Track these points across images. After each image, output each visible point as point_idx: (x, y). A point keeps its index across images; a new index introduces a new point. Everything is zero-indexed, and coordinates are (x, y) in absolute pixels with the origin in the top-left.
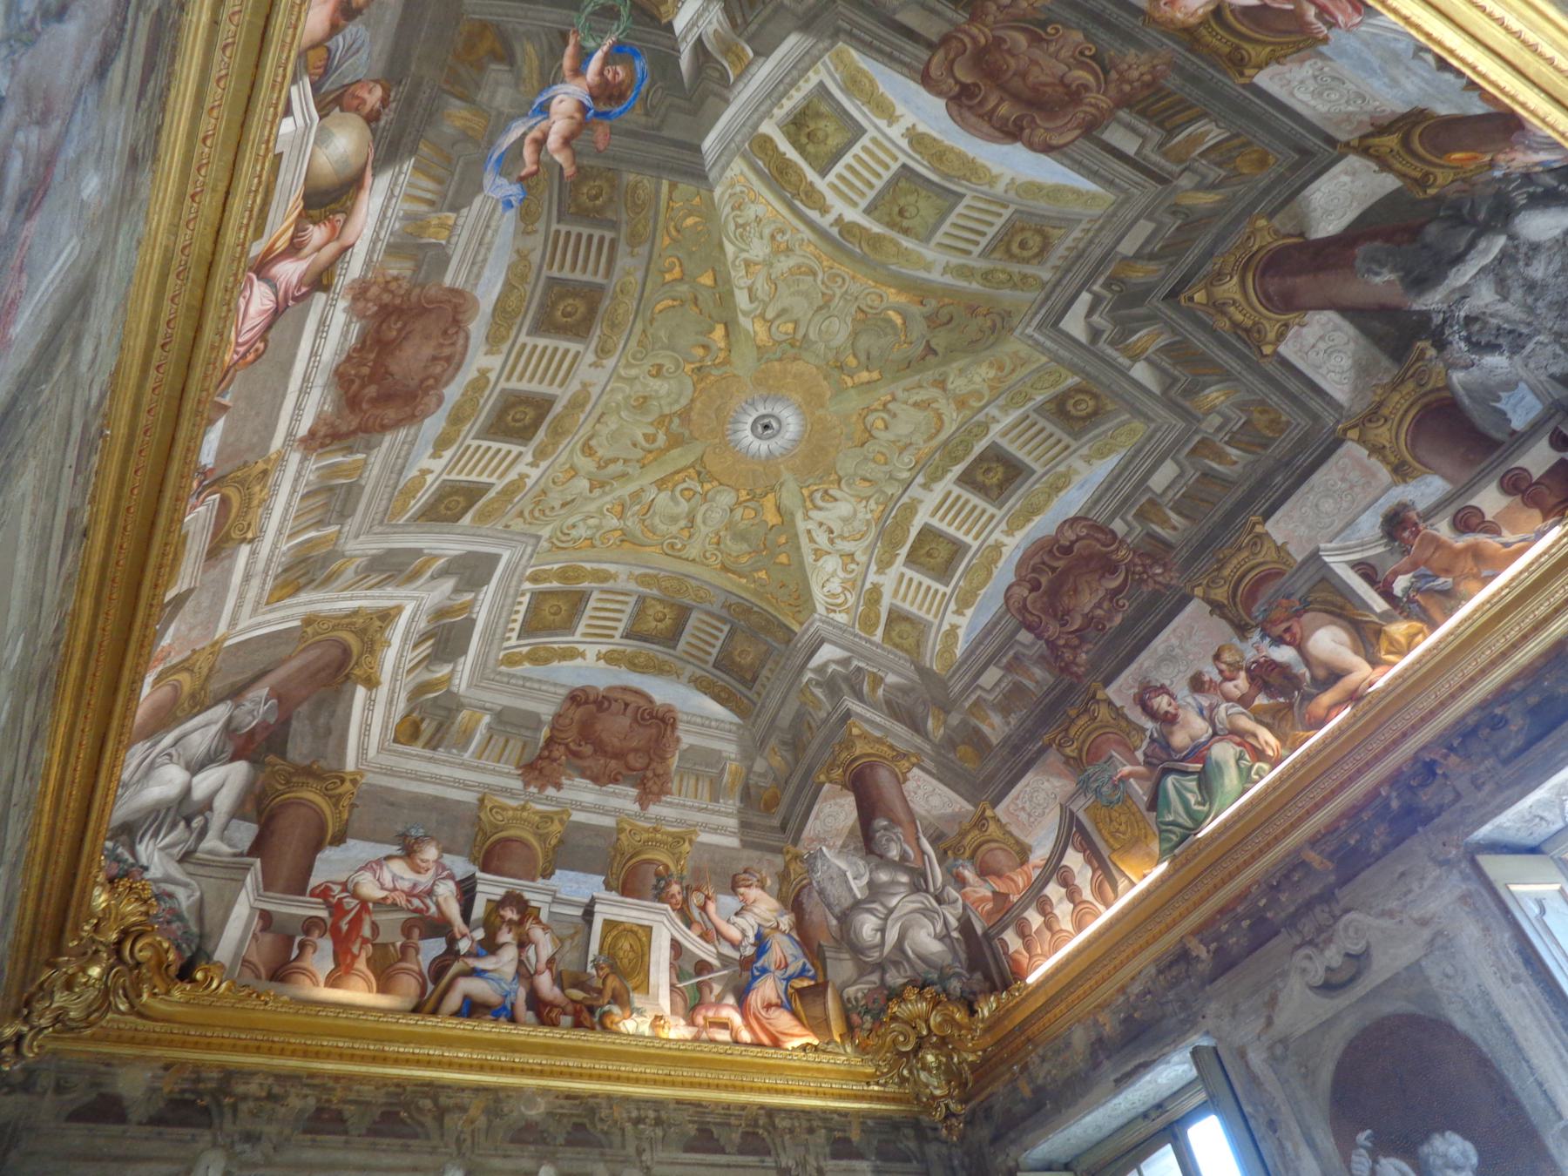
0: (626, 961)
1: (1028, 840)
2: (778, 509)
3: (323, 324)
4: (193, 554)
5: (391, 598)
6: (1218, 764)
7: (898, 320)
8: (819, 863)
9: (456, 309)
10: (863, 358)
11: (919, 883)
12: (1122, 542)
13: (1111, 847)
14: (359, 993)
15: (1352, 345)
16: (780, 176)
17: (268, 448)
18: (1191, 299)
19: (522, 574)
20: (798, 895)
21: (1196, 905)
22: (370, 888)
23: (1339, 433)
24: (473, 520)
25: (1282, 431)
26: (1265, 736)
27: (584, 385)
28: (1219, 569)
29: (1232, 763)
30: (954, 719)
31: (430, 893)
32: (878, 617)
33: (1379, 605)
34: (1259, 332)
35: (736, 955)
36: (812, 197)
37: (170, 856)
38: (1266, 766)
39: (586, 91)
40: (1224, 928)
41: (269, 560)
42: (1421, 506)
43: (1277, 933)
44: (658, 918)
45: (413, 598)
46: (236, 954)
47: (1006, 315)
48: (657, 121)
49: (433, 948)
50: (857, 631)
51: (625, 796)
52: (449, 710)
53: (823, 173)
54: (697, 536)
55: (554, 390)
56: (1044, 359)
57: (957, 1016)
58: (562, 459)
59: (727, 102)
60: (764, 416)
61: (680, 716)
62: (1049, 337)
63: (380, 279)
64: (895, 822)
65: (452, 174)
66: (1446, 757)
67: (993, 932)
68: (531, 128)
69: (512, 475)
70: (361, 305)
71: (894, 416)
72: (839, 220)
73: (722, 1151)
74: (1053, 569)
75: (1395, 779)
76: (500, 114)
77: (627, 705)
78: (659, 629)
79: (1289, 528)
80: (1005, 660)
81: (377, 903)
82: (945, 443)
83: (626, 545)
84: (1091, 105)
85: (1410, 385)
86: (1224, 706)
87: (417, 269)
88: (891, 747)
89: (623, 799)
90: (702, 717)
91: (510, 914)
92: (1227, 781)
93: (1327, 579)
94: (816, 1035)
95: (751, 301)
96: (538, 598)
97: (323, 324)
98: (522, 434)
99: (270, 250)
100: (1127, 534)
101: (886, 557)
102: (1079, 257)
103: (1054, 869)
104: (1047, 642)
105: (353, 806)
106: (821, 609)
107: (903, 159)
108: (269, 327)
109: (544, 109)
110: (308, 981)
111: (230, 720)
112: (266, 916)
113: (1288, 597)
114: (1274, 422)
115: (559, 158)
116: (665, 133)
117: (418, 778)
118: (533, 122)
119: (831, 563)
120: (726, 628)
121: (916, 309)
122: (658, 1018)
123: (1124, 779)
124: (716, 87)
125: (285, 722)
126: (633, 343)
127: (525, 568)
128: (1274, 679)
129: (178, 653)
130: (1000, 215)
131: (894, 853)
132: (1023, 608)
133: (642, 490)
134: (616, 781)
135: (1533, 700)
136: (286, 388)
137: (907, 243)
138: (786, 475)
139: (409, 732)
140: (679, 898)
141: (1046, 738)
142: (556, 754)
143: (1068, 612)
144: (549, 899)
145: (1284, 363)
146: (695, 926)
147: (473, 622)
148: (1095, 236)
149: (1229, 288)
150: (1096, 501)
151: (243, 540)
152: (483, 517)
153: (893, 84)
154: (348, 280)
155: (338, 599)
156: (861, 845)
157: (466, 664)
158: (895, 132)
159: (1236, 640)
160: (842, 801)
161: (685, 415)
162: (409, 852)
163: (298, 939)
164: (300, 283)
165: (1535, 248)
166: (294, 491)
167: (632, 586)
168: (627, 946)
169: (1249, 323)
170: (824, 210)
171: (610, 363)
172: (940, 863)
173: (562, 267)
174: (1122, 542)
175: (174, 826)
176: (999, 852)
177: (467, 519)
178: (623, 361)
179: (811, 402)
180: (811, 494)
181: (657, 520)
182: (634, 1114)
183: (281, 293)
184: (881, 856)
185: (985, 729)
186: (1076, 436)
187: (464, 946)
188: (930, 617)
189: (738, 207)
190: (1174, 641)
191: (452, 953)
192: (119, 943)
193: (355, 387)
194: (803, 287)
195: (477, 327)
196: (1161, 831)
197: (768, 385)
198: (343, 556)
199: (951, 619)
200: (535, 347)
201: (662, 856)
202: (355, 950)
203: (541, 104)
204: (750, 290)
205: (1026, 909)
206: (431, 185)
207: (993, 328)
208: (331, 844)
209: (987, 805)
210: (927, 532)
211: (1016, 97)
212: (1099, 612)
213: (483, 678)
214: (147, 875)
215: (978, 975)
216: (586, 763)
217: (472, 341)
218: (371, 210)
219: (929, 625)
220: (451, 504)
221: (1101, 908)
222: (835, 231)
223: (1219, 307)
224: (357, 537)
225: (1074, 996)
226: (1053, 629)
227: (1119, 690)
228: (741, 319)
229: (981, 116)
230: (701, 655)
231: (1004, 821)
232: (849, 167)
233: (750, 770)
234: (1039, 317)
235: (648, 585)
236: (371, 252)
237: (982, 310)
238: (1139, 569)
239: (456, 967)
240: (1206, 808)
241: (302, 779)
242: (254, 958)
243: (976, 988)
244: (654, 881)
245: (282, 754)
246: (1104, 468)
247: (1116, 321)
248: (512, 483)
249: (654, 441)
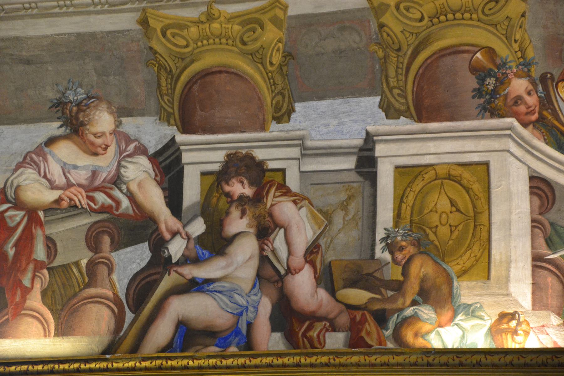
0: (444, 231)
31: (117, 180)
44: (495, 144)
49: (132, 259)
81: (49, 209)
91: (240, 188)
140: (532, 100)
144: (295, 152)
162: (75, 128)
168: (444, 204)
187: (176, 249)
191: (160, 263)
202: (26, 282)
244: (472, 83)
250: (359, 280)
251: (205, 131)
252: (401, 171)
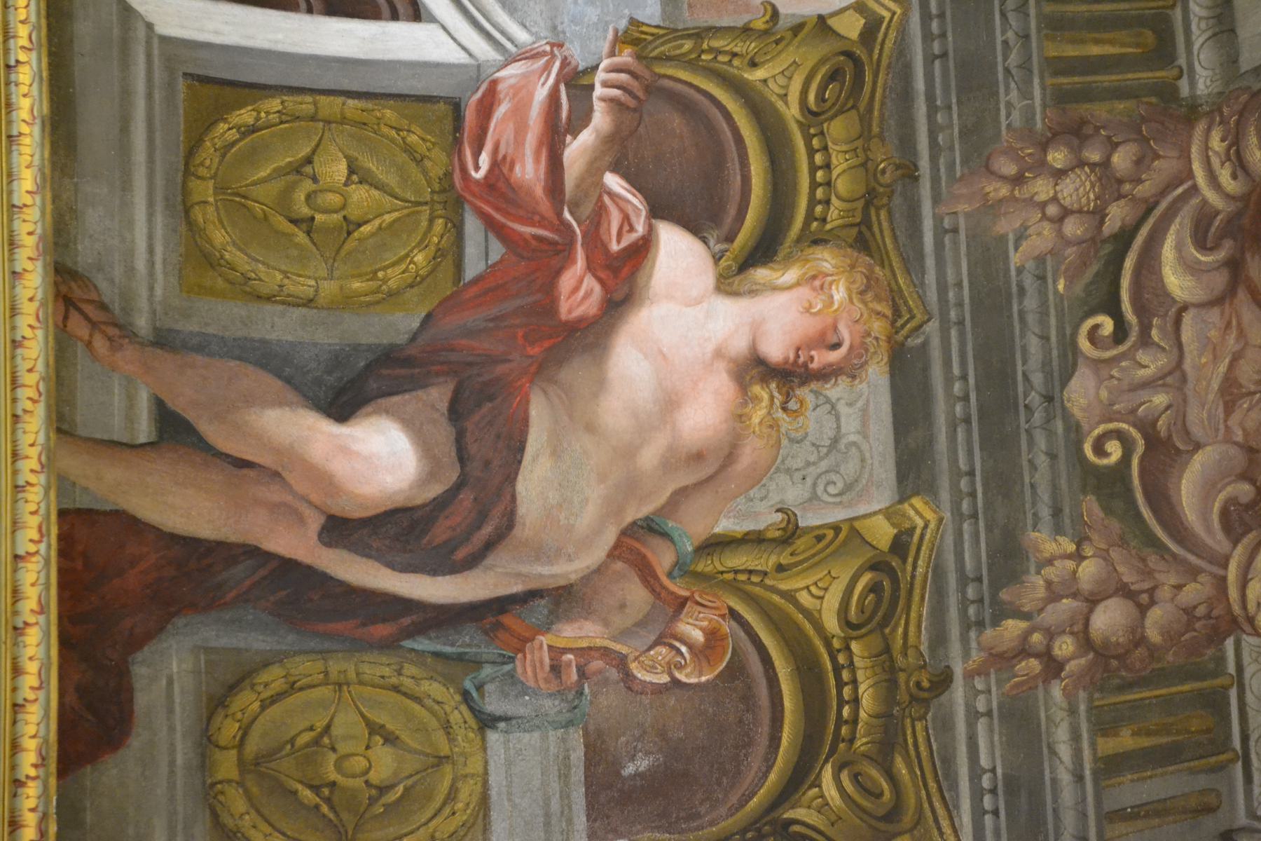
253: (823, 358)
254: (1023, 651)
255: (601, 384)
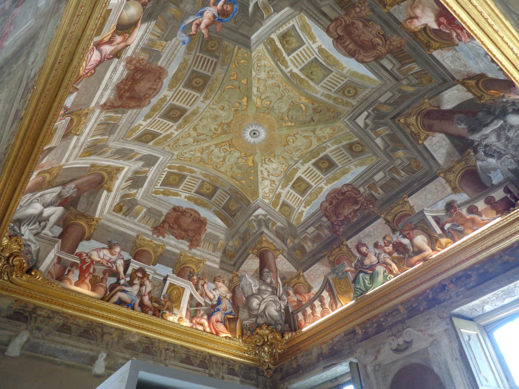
1: (312, 285)
2: (253, 161)
3: (115, 69)
4: (58, 135)
5: (121, 164)
6: (377, 272)
7: (304, 108)
8: (243, 279)
9: (160, 73)
10: (290, 119)
11: (274, 292)
12: (362, 195)
13: (338, 292)
14: (85, 290)
15: (447, 146)
16: (274, 53)
17: (89, 106)
18: (399, 121)
19: (165, 165)
20: (234, 288)
21: (361, 316)
22: (95, 257)
23: (437, 174)
24: (153, 144)
25: (420, 169)
26: (394, 266)
27: (198, 108)
28: (391, 210)
29: (382, 273)
30: (297, 241)
31: (115, 262)
32: (279, 203)
33: (439, 231)
34: (419, 136)
35: (210, 303)
36: (284, 62)
37: (32, 233)
38: (392, 276)
39: (217, 11)
40: (368, 325)
41: (83, 143)
42: (459, 202)
43: (384, 330)
44: (187, 286)
45: (129, 166)
46: (47, 269)
47: (339, 114)
48: (238, 26)
49: (112, 280)
50: (271, 206)
51: (185, 244)
52: (133, 204)
53: (289, 55)
54: (225, 165)
55: (187, 107)
56: (348, 130)
57: (278, 337)
58: (186, 130)
59: (262, 25)
60: (254, 130)
61: (208, 222)
62: (351, 123)
63: (137, 59)
64: (270, 270)
65: (167, 29)
66: (450, 284)
67: (295, 312)
68: (196, 19)
69: (169, 132)
70: (129, 65)
71: (297, 139)
72: (291, 71)
73: (192, 365)
74: (338, 199)
75: (432, 288)
76: (187, 12)
77: (191, 215)
78: (207, 192)
79: (416, 201)
80: (316, 225)
82: (311, 151)
83: (202, 163)
84: (379, 50)
85: (463, 163)
86: (383, 254)
87: (150, 58)
88: (275, 246)
89: (184, 245)
90: (215, 223)
91: (140, 275)
92: (379, 278)
93: (424, 220)
94: (231, 334)
95: (257, 92)
96: (169, 174)
97: (115, 69)
98: (174, 119)
99: (102, 40)
100: (364, 193)
101: (285, 184)
102: (366, 99)
103: (319, 296)
104: (331, 222)
105: (95, 229)
106: (261, 197)
107: (315, 56)
108: (97, 66)
109: (202, 14)
110: (69, 283)
111: (60, 193)
112: (59, 259)
113: (411, 223)
114: (418, 166)
115: (203, 31)
116: (240, 31)
117: (119, 224)
118: (197, 17)
119: (267, 183)
120: (229, 197)
121: (310, 106)
122: (181, 318)
123: (347, 271)
124: (259, 19)
125: (78, 198)
126: (216, 97)
127: (167, 163)
128: (401, 249)
129: (47, 167)
130: (343, 81)
131: (268, 281)
132: (326, 210)
133: (210, 146)
134: (183, 239)
135: (481, 271)
136: (99, 87)
137: (311, 83)
138: (258, 151)
139: (118, 209)
140: (196, 281)
141: (325, 253)
142: (165, 226)
143: (339, 214)
144: (153, 272)
145: (425, 147)
146: (199, 291)
147: (147, 177)
148: (373, 93)
149: (412, 120)
150: (356, 180)
151: (76, 134)
152: (156, 144)
153: (316, 30)
154: (126, 56)
155: (104, 161)
156: (258, 276)
157: (142, 191)
158: (315, 46)
159: (391, 234)
160: (255, 260)
161: (229, 124)
162: (111, 248)
163: (68, 268)
164: (110, 54)
165: (512, 127)
166: (95, 122)
167: (201, 177)
168: (175, 293)
169: (416, 132)
170: (287, 67)
171: (208, 102)
172: (282, 287)
173: (198, 67)
174: (362, 195)
175: (35, 223)
176: (302, 287)
177: (151, 144)
178: (212, 102)
179: (270, 129)
180: (265, 158)
181: (213, 157)
182: (166, 347)
183: (103, 56)
184: (264, 281)
185: (306, 247)
186: (354, 157)
187: (122, 282)
188: (295, 207)
189: (259, 60)
190: (371, 230)
191: (118, 283)
192: (9, 257)
193: (122, 92)
194: (275, 91)
195: (166, 81)
196: (355, 290)
197: (258, 121)
198: (108, 147)
199: (302, 208)
200: (184, 92)
201: (193, 266)
202: (86, 276)
203: (201, 12)
204: (258, 88)
205: (307, 307)
206: (159, 31)
207: (334, 117)
208: (86, 240)
209: (301, 271)
210: (300, 179)
211: (355, 43)
212: (350, 216)
213: (146, 196)
214: (23, 237)
215: (287, 325)
216: (175, 231)
217: (164, 85)
218: (139, 36)
219: (295, 209)
220: (146, 137)
221: (331, 311)
222: (289, 75)
223: (408, 125)
224: (114, 141)
225: (316, 338)
226: (334, 218)
227: (351, 242)
228: (253, 97)
229: (343, 47)
230: (219, 204)
231: (306, 277)
232: (298, 55)
233: (227, 244)
234: (349, 116)
235: (206, 177)
236: (136, 49)
237: (332, 110)
238: (365, 204)
239: (118, 288)
240: (370, 286)
241: (80, 217)
242: (52, 271)
243: (286, 329)
244: (188, 274)
245: (75, 207)
246: (361, 170)
247: (374, 123)
248: (168, 135)
249: (217, 131)
250: (157, 302)
251: (137, 261)
252: (171, 284)
253: (409, 21)
254: (364, 3)
255: (432, 12)
